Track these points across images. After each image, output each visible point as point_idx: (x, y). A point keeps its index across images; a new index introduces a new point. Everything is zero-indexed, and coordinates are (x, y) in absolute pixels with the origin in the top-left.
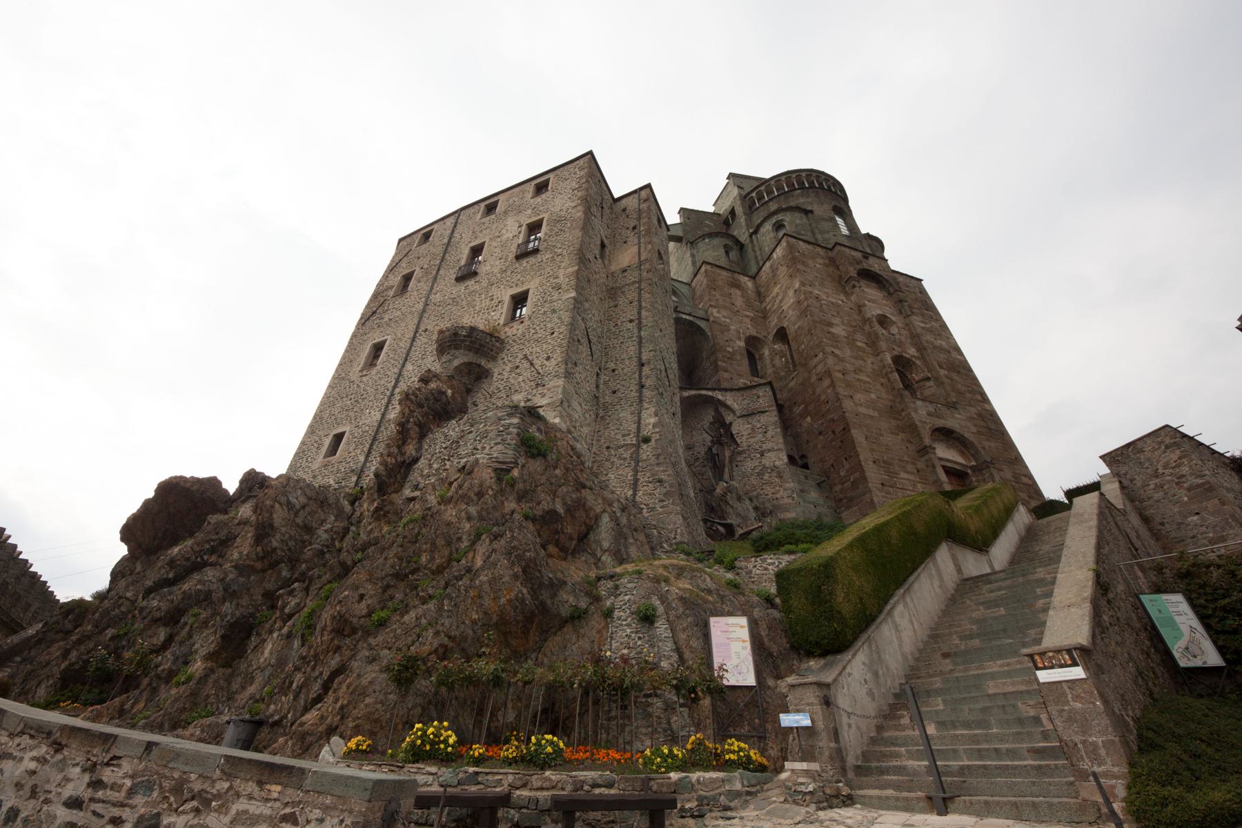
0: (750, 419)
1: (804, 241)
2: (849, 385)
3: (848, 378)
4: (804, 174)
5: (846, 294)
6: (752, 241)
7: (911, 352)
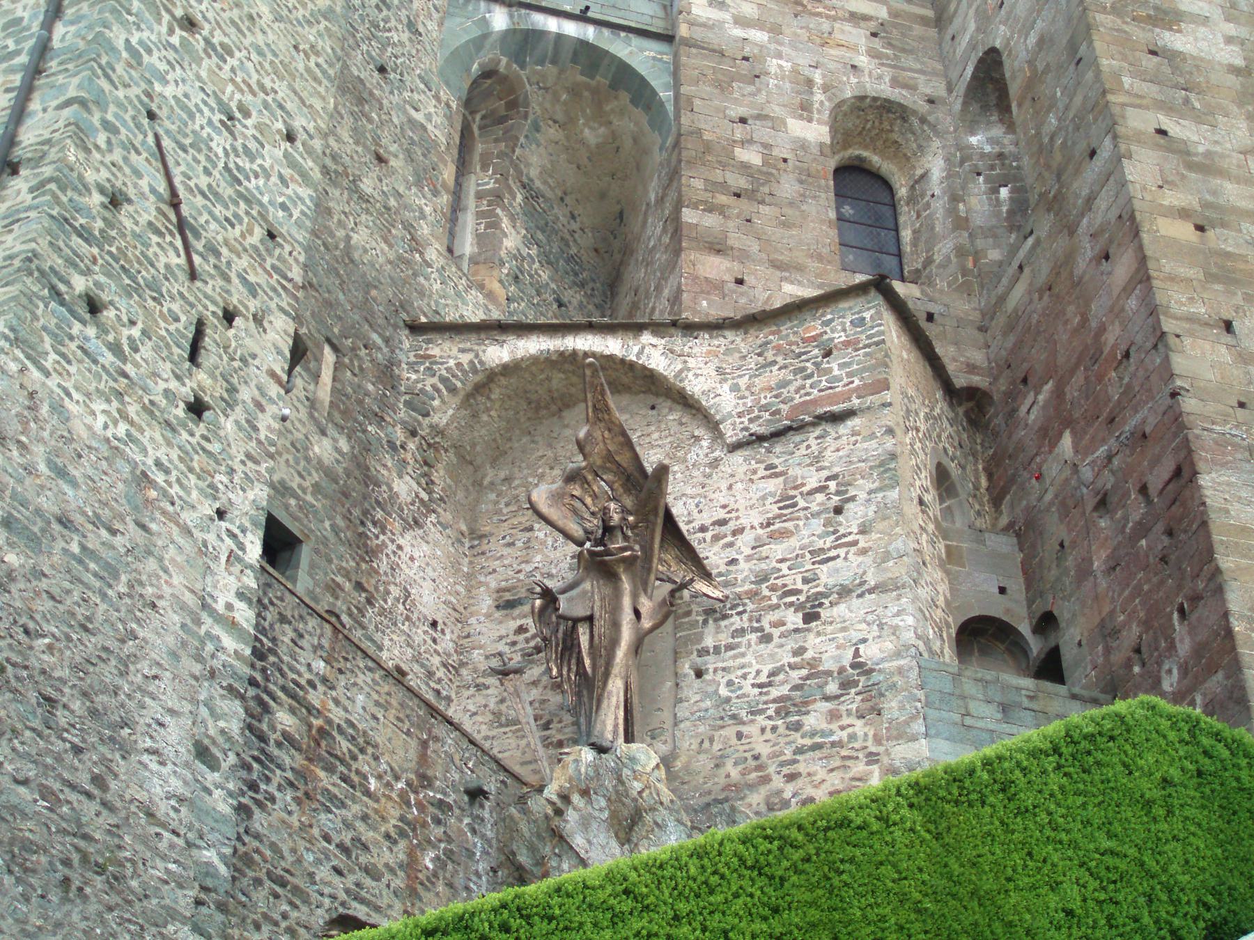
0: (779, 454)
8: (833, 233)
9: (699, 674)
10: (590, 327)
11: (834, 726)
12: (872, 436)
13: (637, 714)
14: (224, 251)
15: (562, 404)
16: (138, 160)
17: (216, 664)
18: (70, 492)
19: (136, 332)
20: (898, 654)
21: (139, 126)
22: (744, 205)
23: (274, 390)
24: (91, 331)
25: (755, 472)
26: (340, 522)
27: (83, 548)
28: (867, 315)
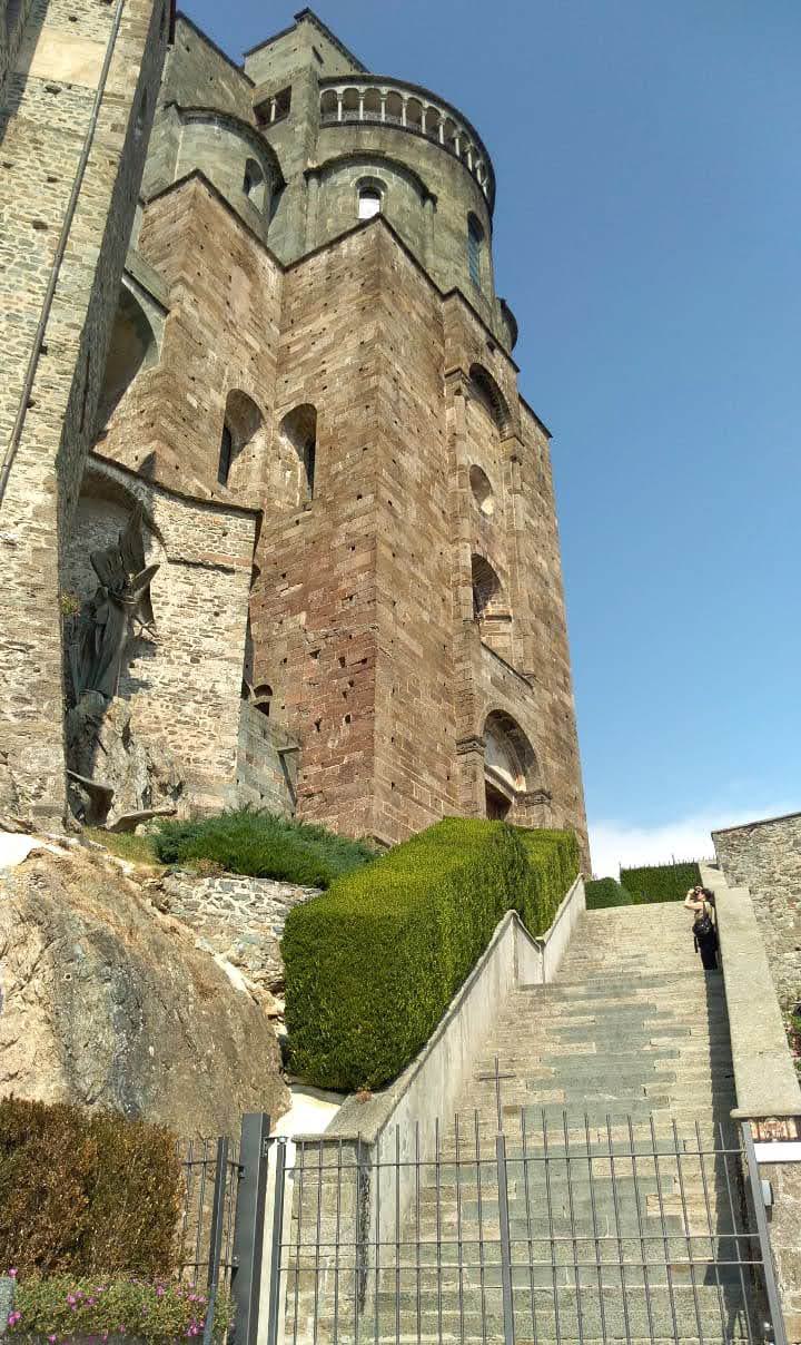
1: (408, 252)
2: (396, 581)
3: (400, 564)
5: (441, 396)
6: (305, 188)
7: (499, 560)
20: (232, 694)
25: (179, 577)
28: (249, 525)
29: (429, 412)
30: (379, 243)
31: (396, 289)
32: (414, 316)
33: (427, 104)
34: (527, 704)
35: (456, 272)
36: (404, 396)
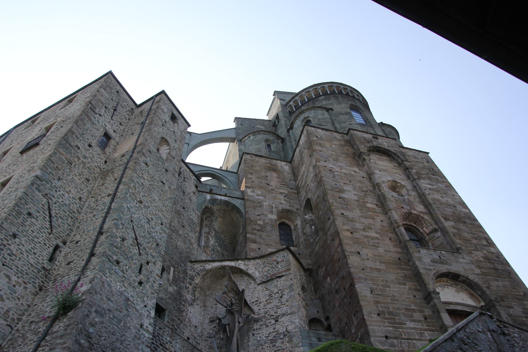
0: (268, 285)
1: (322, 129)
2: (357, 242)
4: (326, 86)
6: (290, 136)
8: (279, 238)
9: (253, 335)
10: (228, 260)
11: (283, 345)
12: (288, 281)
13: (240, 345)
14: (147, 249)
15: (223, 276)
16: (129, 231)
17: (144, 340)
18: (111, 304)
19: (127, 267)
20: (295, 328)
21: (129, 224)
22: (260, 233)
23: (158, 278)
24: (117, 268)
26: (175, 305)
27: (113, 316)
29: (353, 173)
30: (308, 134)
31: (321, 142)
32: (334, 146)
33: (319, 87)
34: (461, 263)
35: (350, 124)
36: (337, 173)
